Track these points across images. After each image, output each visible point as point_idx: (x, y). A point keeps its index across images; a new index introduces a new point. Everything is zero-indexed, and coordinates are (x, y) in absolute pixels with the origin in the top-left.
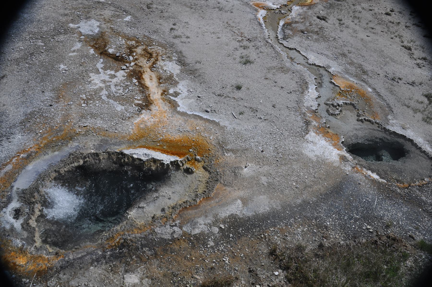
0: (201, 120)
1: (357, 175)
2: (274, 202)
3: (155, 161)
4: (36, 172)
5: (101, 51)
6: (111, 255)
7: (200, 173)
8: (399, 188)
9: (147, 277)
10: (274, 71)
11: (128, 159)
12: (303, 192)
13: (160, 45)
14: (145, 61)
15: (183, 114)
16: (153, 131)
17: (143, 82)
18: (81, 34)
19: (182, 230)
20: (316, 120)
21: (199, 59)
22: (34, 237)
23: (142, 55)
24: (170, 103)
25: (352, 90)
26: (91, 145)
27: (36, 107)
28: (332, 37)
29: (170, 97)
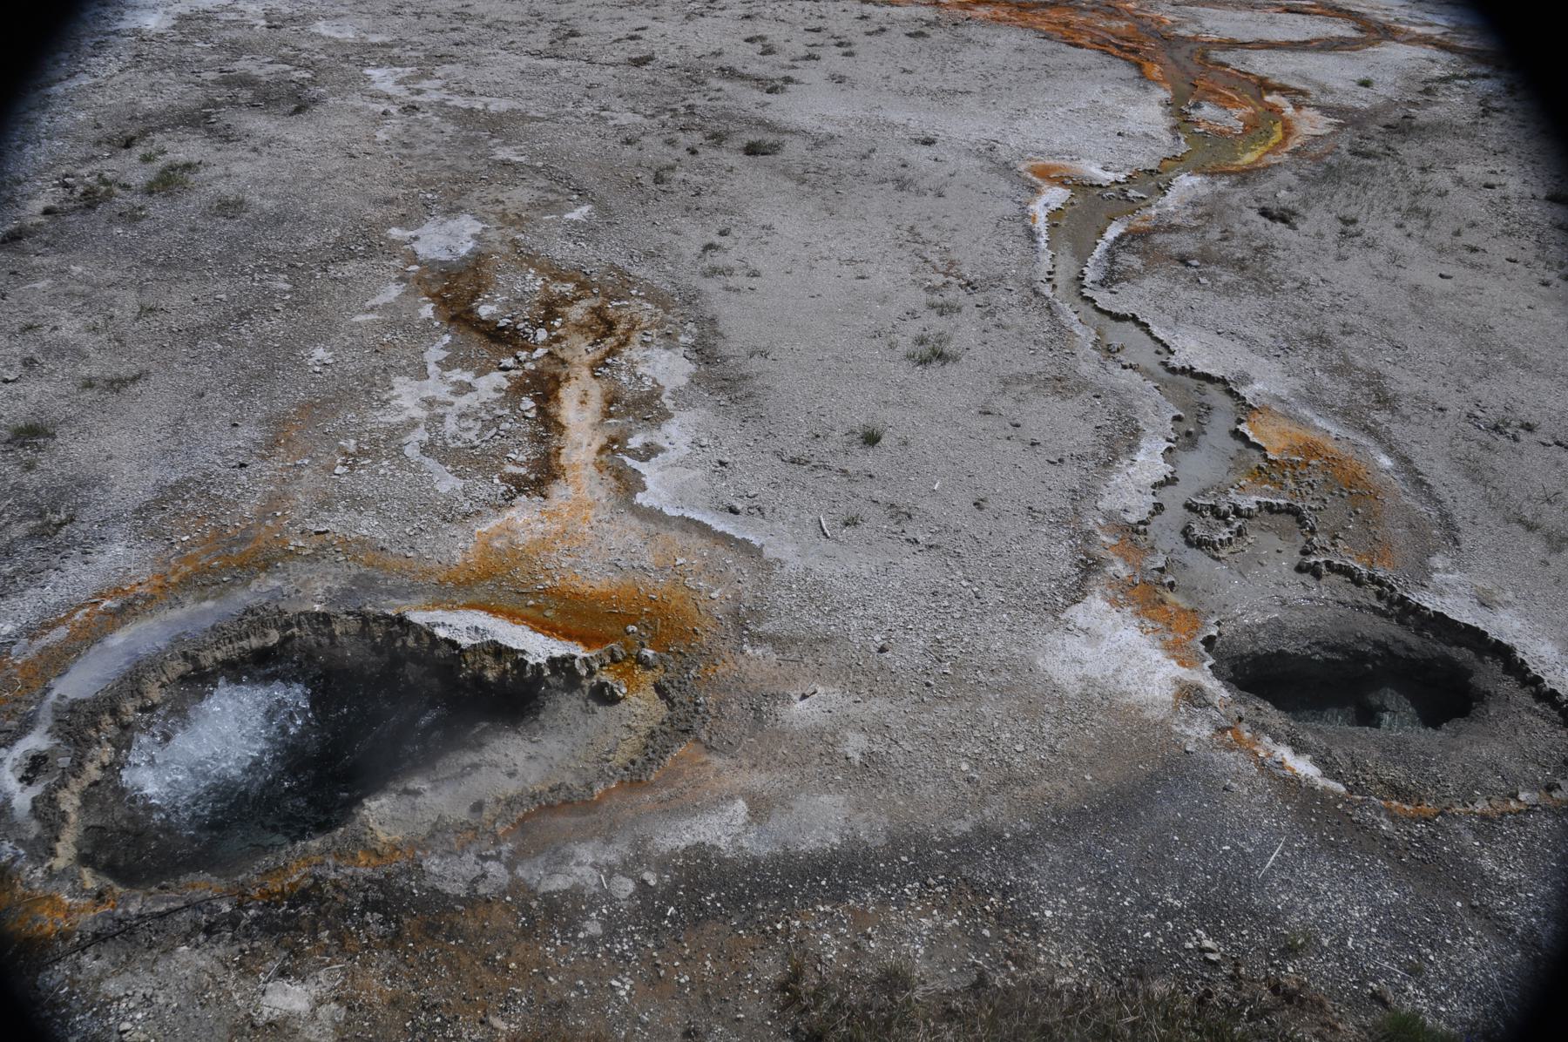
0: (702, 536)
1: (1230, 756)
2: (867, 820)
3: (499, 651)
4: (130, 653)
5: (457, 309)
6: (256, 920)
7: (641, 705)
8: (1393, 818)
9: (337, 999)
10: (1026, 388)
11: (418, 639)
12: (990, 797)
13: (655, 297)
14: (584, 345)
15: (652, 515)
16: (530, 561)
17: (552, 411)
18: (413, 258)
19: (511, 873)
20: (1127, 559)
21: (763, 345)
22: (58, 839)
23: (580, 327)
24: (617, 478)
25: (1313, 462)
26: (320, 591)
27: (199, 468)
28: (1295, 280)
29: (626, 459)
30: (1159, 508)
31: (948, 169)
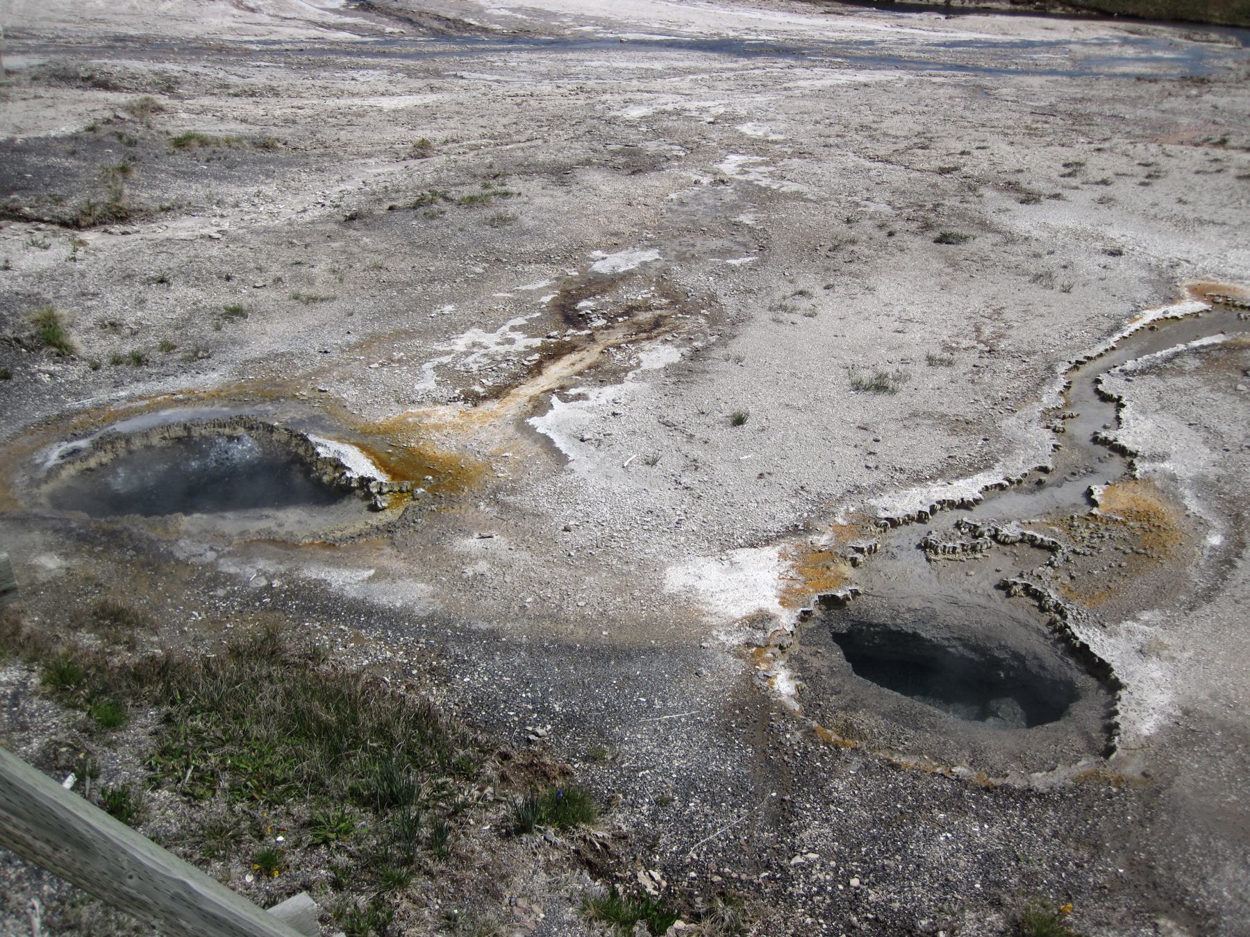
1: (731, 659)
30: (921, 518)
31: (1103, 273)
